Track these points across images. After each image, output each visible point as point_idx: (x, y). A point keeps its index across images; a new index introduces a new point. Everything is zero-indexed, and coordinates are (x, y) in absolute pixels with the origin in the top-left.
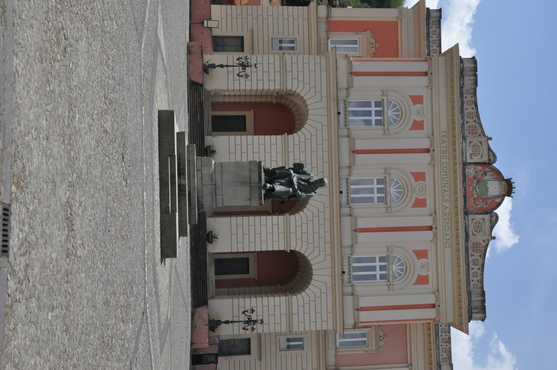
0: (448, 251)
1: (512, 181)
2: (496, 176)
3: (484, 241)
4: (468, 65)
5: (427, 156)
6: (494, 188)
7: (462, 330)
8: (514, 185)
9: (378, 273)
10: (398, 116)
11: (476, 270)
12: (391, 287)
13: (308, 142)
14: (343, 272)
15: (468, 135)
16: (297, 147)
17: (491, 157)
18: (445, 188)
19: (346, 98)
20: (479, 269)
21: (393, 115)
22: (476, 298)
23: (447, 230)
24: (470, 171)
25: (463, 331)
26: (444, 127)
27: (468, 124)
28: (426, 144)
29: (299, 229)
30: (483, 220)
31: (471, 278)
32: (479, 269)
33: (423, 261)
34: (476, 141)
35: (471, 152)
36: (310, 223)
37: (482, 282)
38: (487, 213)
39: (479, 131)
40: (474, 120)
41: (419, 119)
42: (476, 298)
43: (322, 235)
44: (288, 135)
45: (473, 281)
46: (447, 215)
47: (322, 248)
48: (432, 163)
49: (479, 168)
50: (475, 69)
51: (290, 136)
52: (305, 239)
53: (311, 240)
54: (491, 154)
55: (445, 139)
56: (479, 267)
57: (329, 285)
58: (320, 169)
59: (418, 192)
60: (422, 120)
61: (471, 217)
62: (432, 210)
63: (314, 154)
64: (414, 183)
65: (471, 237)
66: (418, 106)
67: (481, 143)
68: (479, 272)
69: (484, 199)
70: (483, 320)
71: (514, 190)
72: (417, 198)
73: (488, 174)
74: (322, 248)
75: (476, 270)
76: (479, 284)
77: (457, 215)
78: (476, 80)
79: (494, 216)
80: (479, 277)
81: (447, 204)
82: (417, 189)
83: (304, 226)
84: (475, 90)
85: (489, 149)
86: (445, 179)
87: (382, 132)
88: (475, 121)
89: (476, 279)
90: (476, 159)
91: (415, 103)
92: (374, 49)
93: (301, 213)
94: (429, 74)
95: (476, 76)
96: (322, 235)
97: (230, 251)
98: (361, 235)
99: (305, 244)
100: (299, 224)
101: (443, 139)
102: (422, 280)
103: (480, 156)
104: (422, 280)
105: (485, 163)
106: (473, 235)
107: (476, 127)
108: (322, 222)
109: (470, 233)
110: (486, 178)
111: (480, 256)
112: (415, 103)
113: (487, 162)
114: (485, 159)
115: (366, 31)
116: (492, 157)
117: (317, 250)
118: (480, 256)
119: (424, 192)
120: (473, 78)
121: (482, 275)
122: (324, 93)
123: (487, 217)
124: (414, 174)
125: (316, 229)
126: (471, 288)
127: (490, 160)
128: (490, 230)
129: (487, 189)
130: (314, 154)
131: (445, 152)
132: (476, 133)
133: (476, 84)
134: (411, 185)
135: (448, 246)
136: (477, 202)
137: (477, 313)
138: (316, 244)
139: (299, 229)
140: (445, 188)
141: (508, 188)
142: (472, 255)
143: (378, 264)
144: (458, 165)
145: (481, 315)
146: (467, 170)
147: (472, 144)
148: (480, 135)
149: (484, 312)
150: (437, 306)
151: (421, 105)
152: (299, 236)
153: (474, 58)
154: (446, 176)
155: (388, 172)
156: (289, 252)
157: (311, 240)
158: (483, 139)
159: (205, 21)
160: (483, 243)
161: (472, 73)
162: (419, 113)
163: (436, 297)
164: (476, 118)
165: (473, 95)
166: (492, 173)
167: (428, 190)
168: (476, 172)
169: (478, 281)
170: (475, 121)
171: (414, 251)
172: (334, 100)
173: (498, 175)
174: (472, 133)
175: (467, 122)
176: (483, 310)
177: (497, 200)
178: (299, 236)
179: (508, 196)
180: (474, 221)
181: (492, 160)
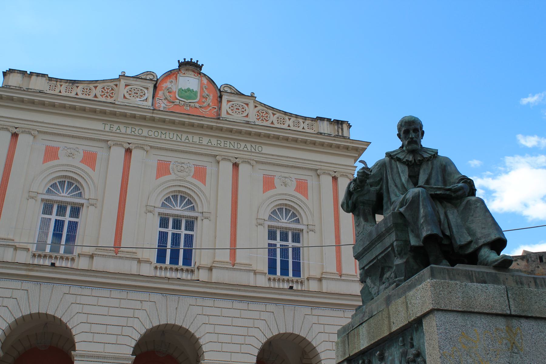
0: (266, 150)
1: (182, 60)
2: (174, 77)
3: (256, 107)
4: (15, 80)
5: (135, 153)
6: (189, 82)
7: (364, 149)
8: (188, 59)
9: (290, 244)
10: (70, 184)
11: (291, 123)
12: (310, 227)
13: (92, 319)
15: (113, 99)
16: (98, 338)
17: (148, 77)
19: (30, 254)
20: (290, 119)
21: (67, 191)
22: (325, 128)
23: (239, 146)
24: (163, 105)
25: (365, 149)
26: (99, 126)
27: (98, 95)
28: (118, 153)
29: (226, 347)
30: (229, 101)
31: (300, 129)
32: (290, 119)
33: (277, 182)
34: (122, 90)
35: (138, 99)
36: (219, 329)
37: (305, 118)
38: (221, 97)
39: (112, 84)
40: (94, 88)
41: (80, 156)
42: (325, 128)
43: (236, 313)
44: (75, 350)
45: (303, 128)
46: (219, 142)
47: (255, 315)
49: (160, 93)
50: (24, 73)
51: (78, 346)
52: (241, 340)
53: (243, 331)
54: (143, 77)
56: (287, 118)
57: (307, 310)
58: (138, 305)
59: (185, 174)
60: (82, 154)
61: (224, 114)
62: (211, 159)
63: (113, 312)
64: (172, 177)
65: (250, 119)
66: (60, 153)
67: (126, 85)
68: (293, 119)
69: (202, 97)
70: (349, 126)
71: (194, 60)
72: (193, 177)
73: (170, 86)
74: (255, 315)
75: (291, 123)
76: (307, 122)
77: (221, 129)
78: (38, 75)
79: (226, 89)
80: (301, 121)
82: (179, 174)
83: (223, 338)
84: (51, 79)
85: (136, 77)
86: (171, 137)
87: (91, 208)
88: (96, 87)
89: (302, 125)
90: (149, 94)
91: (56, 157)
93: (201, 341)
95: (32, 73)
96: (236, 313)
98: (241, 257)
99: (249, 340)
100: (217, 347)
101: (115, 129)
102: (302, 187)
103: (146, 91)
104: (302, 187)
105: (155, 87)
106: (247, 116)
107: (104, 88)
108: (217, 312)
109: (246, 119)
110: (174, 89)
111: (274, 114)
112: (56, 157)
113: (155, 83)
117: (257, 323)
118: (274, 114)
119: (186, 167)
120: (34, 78)
121: (297, 116)
123: (225, 98)
124: (159, 174)
125: (228, 321)
126: (312, 131)
127: (151, 80)
128: (242, 96)
129: (188, 90)
130: (113, 312)
131: (133, 130)
132: (112, 89)
133: (44, 75)
134: (174, 180)
135: (260, 149)
136: (205, 104)
137: (342, 130)
138: (249, 323)
139: (226, 347)
141: (190, 66)
142: (272, 123)
143: (278, 243)
144: (154, 115)
145: (345, 126)
146: (162, 109)
147: (127, 96)
148: (116, 85)
149: (342, 122)
150: (336, 174)
151: (60, 151)
152: (236, 348)
153: (5, 74)
154: (167, 134)
155: (152, 209)
157: (243, 331)
158: (123, 82)
160: (257, 109)
161: (26, 79)
162: (71, 155)
163: (324, 173)
164: (91, 86)
165: (58, 83)
166: (169, 80)
167: (183, 161)
168: (166, 99)
169: (304, 122)
170: (96, 87)
173: (170, 74)
174: (112, 93)
175: (96, 96)
176: (339, 123)
177: (205, 81)
178: (236, 348)
179: (201, 70)
180: (230, 112)
181: (151, 77)
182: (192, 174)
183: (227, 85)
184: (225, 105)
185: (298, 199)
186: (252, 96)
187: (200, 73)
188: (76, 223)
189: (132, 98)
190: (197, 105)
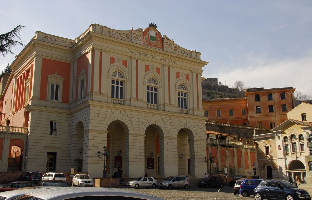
0: (178, 62)
1: (150, 24)
8: (153, 24)
14: (186, 113)
18: (153, 57)
48: (142, 60)
55: (132, 51)
67: (134, 34)
81: (160, 58)
85: (137, 30)
90: (141, 38)
91: (114, 62)
92: (59, 75)
94: (101, 51)
97: (207, 168)
114: (141, 34)
115: (48, 78)
116: (140, 30)
122: (110, 110)
123: (165, 41)
140: (153, 57)
141: (153, 26)
156: (178, 138)
158: (133, 32)
159: (71, 176)
162: (118, 61)
171: (177, 79)
172: (115, 106)
173: (147, 30)
182: (156, 71)
183: (165, 36)
184: (165, 45)
185: (186, 81)
186: (173, 41)
187: (156, 30)
188: (122, 88)
189: (136, 39)
190: (156, 43)
